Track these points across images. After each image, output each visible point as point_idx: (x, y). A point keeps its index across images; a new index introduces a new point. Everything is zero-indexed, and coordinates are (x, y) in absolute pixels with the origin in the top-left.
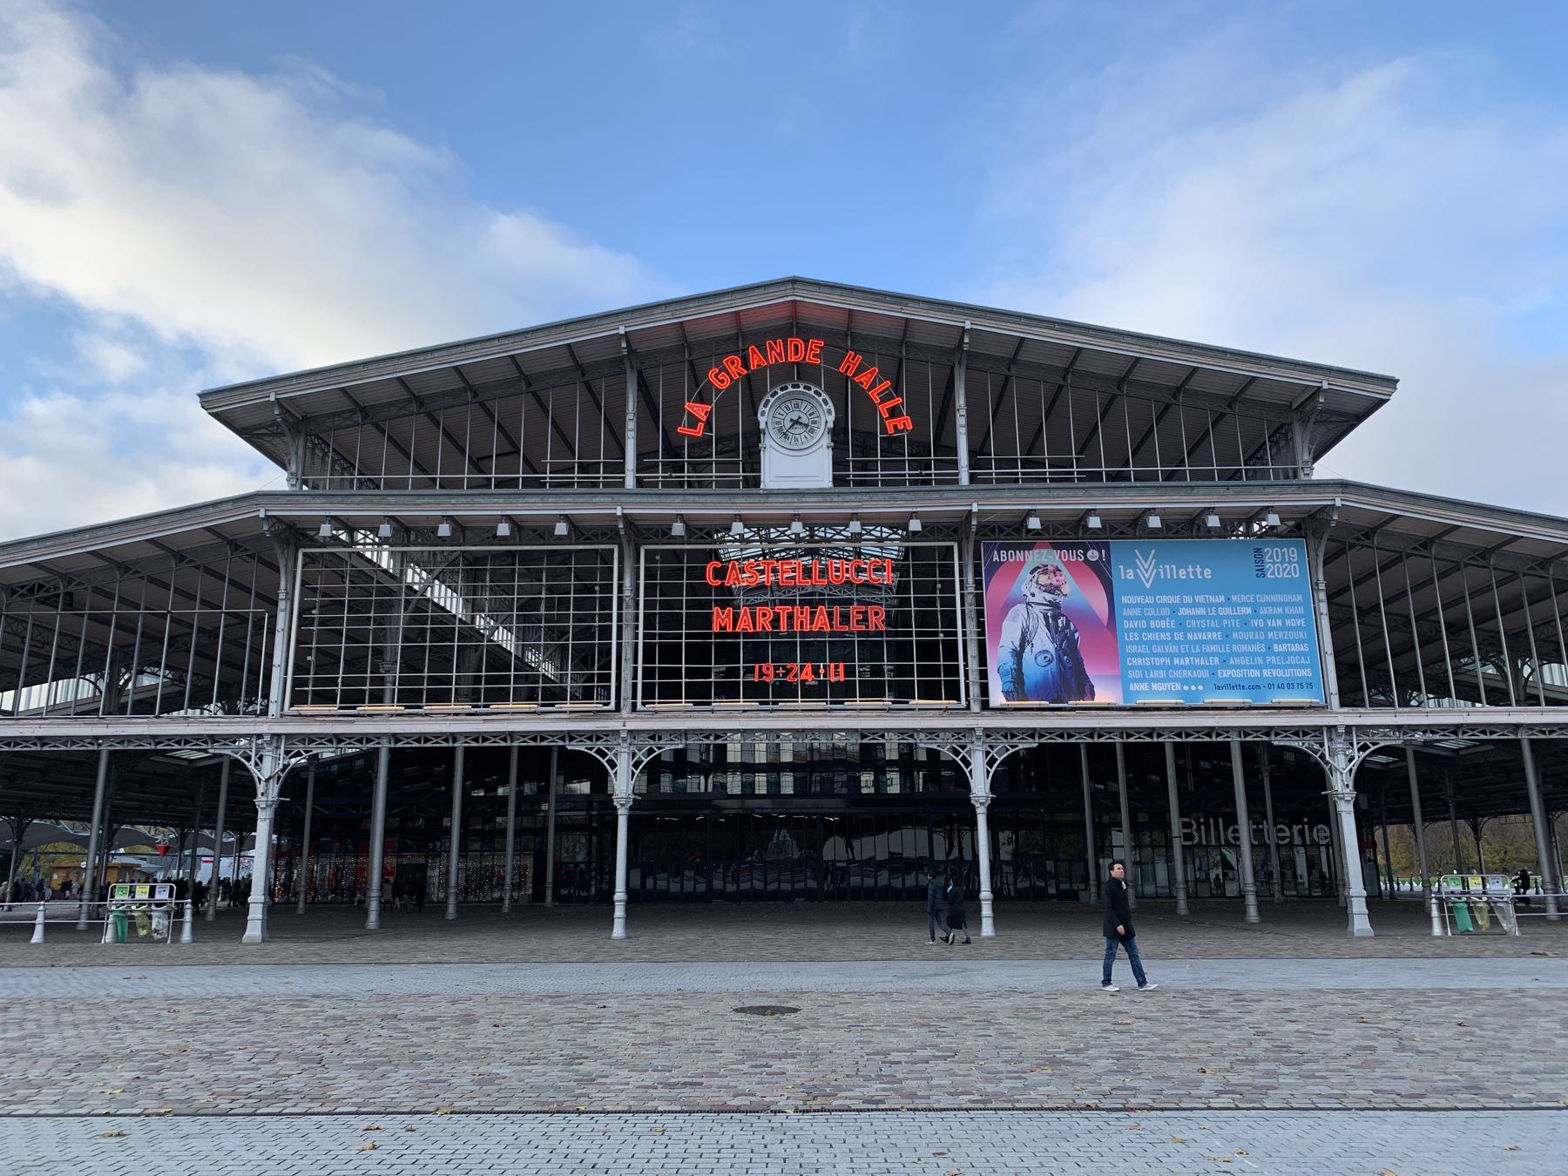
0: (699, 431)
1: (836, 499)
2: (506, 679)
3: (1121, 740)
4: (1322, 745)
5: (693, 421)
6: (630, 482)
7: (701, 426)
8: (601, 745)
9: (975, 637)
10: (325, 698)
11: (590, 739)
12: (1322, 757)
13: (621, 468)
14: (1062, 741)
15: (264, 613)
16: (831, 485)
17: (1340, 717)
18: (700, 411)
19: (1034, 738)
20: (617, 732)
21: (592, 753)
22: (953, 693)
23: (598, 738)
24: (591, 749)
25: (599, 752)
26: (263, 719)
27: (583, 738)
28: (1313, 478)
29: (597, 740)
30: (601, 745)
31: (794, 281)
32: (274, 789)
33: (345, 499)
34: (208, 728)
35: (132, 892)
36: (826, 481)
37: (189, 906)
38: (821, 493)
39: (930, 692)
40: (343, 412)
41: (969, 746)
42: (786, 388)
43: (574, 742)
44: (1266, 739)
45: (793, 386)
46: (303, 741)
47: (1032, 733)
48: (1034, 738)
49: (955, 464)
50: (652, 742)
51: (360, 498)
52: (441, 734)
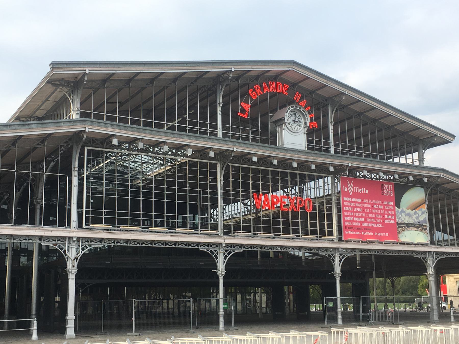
1: (309, 155)
2: (126, 215)
3: (261, 250)
4: (426, 258)
6: (220, 134)
8: (212, 249)
10: (99, 221)
11: (208, 246)
13: (216, 127)
14: (186, 247)
15: (67, 176)
17: (433, 248)
19: (241, 248)
20: (221, 244)
21: (209, 252)
22: (331, 234)
23: (211, 246)
24: (208, 250)
25: (211, 251)
26: (68, 229)
27: (205, 246)
28: (424, 165)
29: (210, 247)
30: (212, 249)
31: (294, 63)
32: (76, 264)
33: (126, 128)
34: (46, 233)
37: (35, 322)
40: (97, 80)
41: (334, 254)
42: (293, 107)
43: (202, 247)
44: (317, 252)
45: (299, 108)
48: (241, 248)
50: (231, 249)
51: (133, 129)
52: (249, 245)
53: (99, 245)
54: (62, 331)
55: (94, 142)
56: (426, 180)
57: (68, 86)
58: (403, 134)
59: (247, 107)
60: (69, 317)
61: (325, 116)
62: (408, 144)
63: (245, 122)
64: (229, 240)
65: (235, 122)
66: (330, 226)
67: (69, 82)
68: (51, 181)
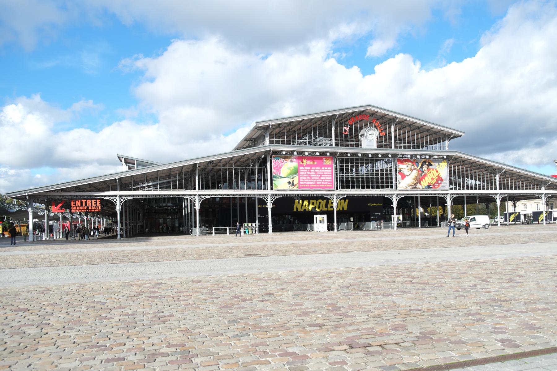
0: (347, 133)
5: (345, 131)
7: (347, 132)
9: (395, 177)
12: (447, 199)
16: (376, 148)
18: (347, 129)
22: (391, 187)
26: (267, 191)
35: (248, 225)
36: (375, 146)
38: (375, 150)
39: (387, 187)
46: (203, 195)
47: (403, 194)
49: (391, 143)
53: (281, 197)
54: (267, 231)
55: (276, 152)
56: (445, 157)
57: (264, 129)
58: (436, 133)
59: (347, 129)
60: (269, 226)
61: (390, 127)
62: (439, 139)
63: (346, 136)
64: (339, 192)
65: (341, 136)
66: (391, 182)
67: (264, 127)
68: (259, 171)
